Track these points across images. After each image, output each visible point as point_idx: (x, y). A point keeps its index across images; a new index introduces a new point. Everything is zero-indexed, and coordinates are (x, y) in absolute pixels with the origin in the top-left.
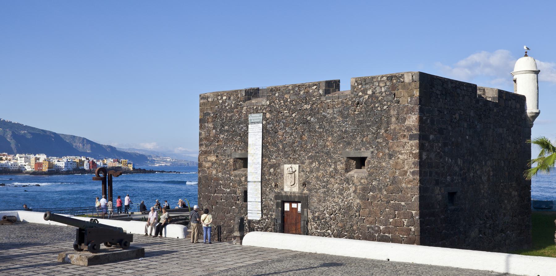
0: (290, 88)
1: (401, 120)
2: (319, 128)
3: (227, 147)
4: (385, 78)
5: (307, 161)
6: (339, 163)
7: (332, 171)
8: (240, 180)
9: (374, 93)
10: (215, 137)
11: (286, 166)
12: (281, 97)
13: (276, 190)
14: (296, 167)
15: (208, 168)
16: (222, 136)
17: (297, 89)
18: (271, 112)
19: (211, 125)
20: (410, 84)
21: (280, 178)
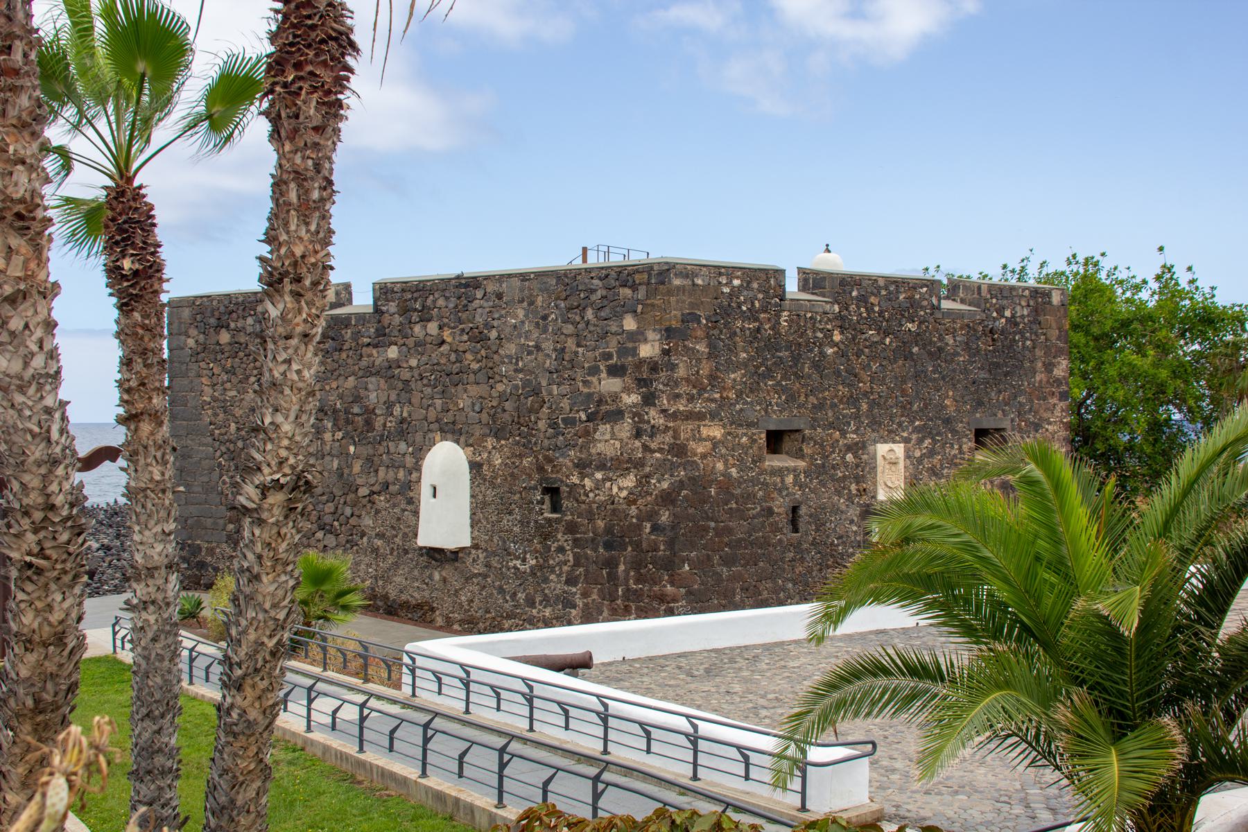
0: (881, 283)
1: (1049, 367)
2: (934, 372)
3: (746, 403)
4: (1027, 293)
5: (914, 437)
6: (965, 440)
7: (955, 456)
8: (783, 481)
9: (1013, 316)
10: (712, 377)
11: (882, 449)
12: (863, 299)
13: (865, 499)
14: (899, 449)
15: (704, 456)
16: (732, 376)
17: (892, 288)
18: (842, 329)
19: (702, 348)
20: (1058, 307)
21: (869, 473)
